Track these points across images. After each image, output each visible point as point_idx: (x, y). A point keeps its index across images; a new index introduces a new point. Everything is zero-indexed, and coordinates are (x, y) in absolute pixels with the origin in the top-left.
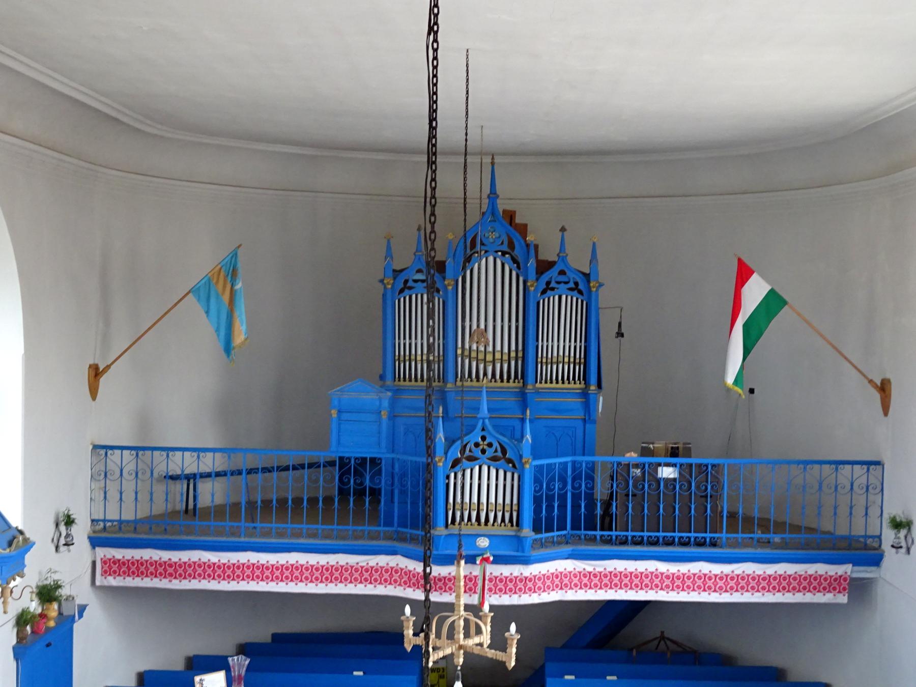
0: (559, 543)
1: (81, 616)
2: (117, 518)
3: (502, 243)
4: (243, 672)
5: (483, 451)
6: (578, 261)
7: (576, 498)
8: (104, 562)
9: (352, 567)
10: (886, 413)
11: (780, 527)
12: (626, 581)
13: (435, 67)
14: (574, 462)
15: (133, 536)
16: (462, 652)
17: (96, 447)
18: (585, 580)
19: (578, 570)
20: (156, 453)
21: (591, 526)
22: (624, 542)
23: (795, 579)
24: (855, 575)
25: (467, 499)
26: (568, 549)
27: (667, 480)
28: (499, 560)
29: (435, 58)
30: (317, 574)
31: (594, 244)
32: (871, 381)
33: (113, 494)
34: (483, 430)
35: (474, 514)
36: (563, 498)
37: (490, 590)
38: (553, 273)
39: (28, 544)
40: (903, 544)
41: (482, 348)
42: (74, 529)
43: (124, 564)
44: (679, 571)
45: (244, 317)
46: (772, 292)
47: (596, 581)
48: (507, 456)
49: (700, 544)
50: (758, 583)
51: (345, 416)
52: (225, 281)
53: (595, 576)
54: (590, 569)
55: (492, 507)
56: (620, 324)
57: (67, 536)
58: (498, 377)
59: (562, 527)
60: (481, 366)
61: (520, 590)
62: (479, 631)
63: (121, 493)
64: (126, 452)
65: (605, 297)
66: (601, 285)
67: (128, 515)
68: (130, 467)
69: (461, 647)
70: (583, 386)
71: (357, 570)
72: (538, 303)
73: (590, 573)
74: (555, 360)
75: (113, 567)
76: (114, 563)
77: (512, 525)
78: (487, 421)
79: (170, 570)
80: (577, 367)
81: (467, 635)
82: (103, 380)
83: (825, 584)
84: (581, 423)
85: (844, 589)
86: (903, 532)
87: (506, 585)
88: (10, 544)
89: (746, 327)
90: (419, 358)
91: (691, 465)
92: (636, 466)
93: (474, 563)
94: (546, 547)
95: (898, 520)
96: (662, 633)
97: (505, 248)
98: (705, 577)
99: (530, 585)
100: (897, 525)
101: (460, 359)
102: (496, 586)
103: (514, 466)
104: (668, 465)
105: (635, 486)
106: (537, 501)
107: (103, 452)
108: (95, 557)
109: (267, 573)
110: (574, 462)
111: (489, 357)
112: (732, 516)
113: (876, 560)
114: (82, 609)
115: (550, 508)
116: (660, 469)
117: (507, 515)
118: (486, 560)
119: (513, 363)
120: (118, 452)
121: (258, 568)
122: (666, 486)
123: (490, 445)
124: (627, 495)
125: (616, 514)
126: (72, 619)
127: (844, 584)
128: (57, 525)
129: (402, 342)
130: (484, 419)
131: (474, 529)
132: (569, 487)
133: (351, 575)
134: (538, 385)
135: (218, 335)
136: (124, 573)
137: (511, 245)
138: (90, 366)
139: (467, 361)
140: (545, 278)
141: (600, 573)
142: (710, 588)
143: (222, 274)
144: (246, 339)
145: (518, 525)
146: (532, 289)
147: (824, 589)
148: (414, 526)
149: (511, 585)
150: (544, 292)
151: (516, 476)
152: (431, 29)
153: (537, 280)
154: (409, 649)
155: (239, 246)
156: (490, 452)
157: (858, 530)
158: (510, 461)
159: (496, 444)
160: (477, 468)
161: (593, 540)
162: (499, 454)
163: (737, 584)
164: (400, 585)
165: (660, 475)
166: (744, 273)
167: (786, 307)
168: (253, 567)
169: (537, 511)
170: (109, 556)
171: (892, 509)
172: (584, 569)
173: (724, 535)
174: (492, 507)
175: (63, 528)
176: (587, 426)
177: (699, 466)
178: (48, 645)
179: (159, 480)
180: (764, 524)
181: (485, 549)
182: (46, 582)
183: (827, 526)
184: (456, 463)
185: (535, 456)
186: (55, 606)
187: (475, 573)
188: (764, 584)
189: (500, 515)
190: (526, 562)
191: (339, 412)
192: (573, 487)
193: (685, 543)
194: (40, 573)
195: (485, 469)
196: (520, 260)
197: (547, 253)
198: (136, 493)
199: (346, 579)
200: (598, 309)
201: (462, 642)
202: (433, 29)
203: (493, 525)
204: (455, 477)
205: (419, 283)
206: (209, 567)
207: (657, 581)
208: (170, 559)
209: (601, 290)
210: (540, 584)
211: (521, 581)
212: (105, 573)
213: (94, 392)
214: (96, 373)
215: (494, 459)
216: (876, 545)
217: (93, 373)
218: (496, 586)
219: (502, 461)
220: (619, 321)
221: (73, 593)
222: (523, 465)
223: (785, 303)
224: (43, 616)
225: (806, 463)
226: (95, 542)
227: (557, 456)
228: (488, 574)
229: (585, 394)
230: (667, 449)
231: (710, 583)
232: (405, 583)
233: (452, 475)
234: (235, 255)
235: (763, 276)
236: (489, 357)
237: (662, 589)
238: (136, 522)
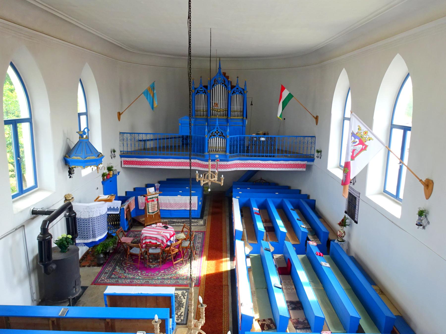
0: (236, 156)
1: (118, 174)
2: (127, 150)
3: (222, 81)
4: (159, 187)
5: (217, 134)
6: (241, 86)
7: (240, 145)
10: (317, 125)
11: (290, 152)
12: (252, 165)
13: (190, 28)
14: (240, 137)
15: (130, 155)
16: (210, 182)
17: (120, 133)
18: (242, 165)
20: (136, 134)
21: (244, 152)
22: (252, 156)
23: (293, 165)
24: (308, 164)
25: (213, 146)
26: (238, 158)
27: (263, 141)
28: (221, 160)
29: (190, 25)
31: (245, 81)
32: (313, 116)
33: (125, 145)
34: (217, 128)
35: (215, 149)
36: (237, 145)
37: (219, 168)
38: (235, 89)
39: (103, 156)
40: (319, 156)
41: (217, 108)
42: (116, 153)
43: (129, 162)
45: (156, 100)
46: (290, 93)
47: (245, 165)
48: (223, 135)
49: (270, 156)
50: (284, 166)
51: (182, 125)
52: (151, 91)
54: (243, 163)
56: (252, 102)
57: (114, 155)
58: (221, 115)
59: (237, 152)
60: (217, 113)
61: (226, 168)
62: (214, 177)
63: (127, 144)
64: (128, 134)
65: (248, 95)
66: (247, 92)
67: (129, 150)
68: (129, 138)
69: (210, 181)
70: (242, 118)
71: (186, 163)
72: (231, 96)
74: (235, 111)
75: (126, 163)
76: (126, 161)
78: (218, 126)
79: (140, 163)
81: (211, 178)
82: (122, 116)
83: (300, 166)
84: (241, 127)
85: (305, 167)
86: (319, 153)
87: (223, 167)
88: (98, 156)
89: (283, 102)
90: (201, 110)
91: (268, 137)
92: (255, 137)
93: (215, 161)
94: (233, 157)
95: (318, 150)
96: (261, 178)
97: (223, 82)
98: (271, 164)
99: (229, 166)
100: (318, 152)
101: (211, 111)
103: (225, 137)
104: (263, 137)
105: (255, 142)
106: (230, 146)
107: (122, 134)
109: (164, 164)
110: (240, 138)
111: (219, 110)
112: (278, 150)
113: (313, 160)
114: (119, 173)
115: (234, 148)
116: (261, 138)
117: (223, 150)
118: (218, 160)
119: (225, 112)
120: (126, 134)
121: (162, 163)
122: (262, 143)
123: (219, 132)
124: (253, 145)
126: (116, 175)
127: (305, 166)
128: (111, 152)
129: (197, 107)
130: (217, 126)
131: (215, 153)
132: (238, 143)
133: (185, 164)
134: (231, 117)
135: (150, 104)
136: (129, 164)
137: (224, 81)
138: (118, 112)
139: (213, 111)
140: (233, 90)
142: (272, 167)
143: (150, 89)
144: (157, 105)
145: (226, 152)
146: (230, 93)
147: (300, 167)
148: (200, 152)
150: (233, 94)
151: (225, 140)
152: (189, 17)
153: (231, 90)
154: (197, 181)
155: (155, 82)
156: (219, 134)
157: (309, 153)
158: (224, 136)
159: (220, 132)
160: (216, 138)
161: (244, 156)
162: (221, 134)
163: (279, 166)
165: (261, 140)
166: (283, 89)
167: (293, 98)
168: (161, 162)
169: (230, 148)
171: (317, 148)
173: (276, 154)
175: (113, 153)
176: (244, 128)
177: (270, 137)
178: (111, 181)
179: (137, 141)
180: (286, 152)
181: (217, 158)
182: (109, 166)
183: (301, 152)
184: (211, 136)
185: (230, 135)
186: (112, 172)
188: (285, 166)
189: (221, 149)
190: (228, 161)
191: (181, 124)
192: (239, 143)
193: (267, 156)
194: (108, 164)
195: (218, 138)
196: (227, 85)
197: (234, 84)
198: (131, 144)
200: (246, 98)
201: (210, 179)
202: (189, 17)
205: (201, 91)
206: (150, 162)
207: (260, 165)
209: (247, 93)
210: (231, 166)
211: (226, 165)
212: (124, 164)
213: (119, 119)
214: (119, 114)
215: (220, 136)
216: (313, 157)
217: (119, 114)
219: (222, 136)
221: (116, 169)
222: (227, 137)
223: (293, 96)
224: (109, 174)
225: (297, 137)
226: (121, 156)
227: (236, 135)
228: (218, 164)
229: (243, 120)
230: (263, 134)
231: (272, 166)
232: (198, 166)
233: (209, 140)
234: (154, 84)
235: (288, 90)
236: (219, 110)
238: (131, 152)
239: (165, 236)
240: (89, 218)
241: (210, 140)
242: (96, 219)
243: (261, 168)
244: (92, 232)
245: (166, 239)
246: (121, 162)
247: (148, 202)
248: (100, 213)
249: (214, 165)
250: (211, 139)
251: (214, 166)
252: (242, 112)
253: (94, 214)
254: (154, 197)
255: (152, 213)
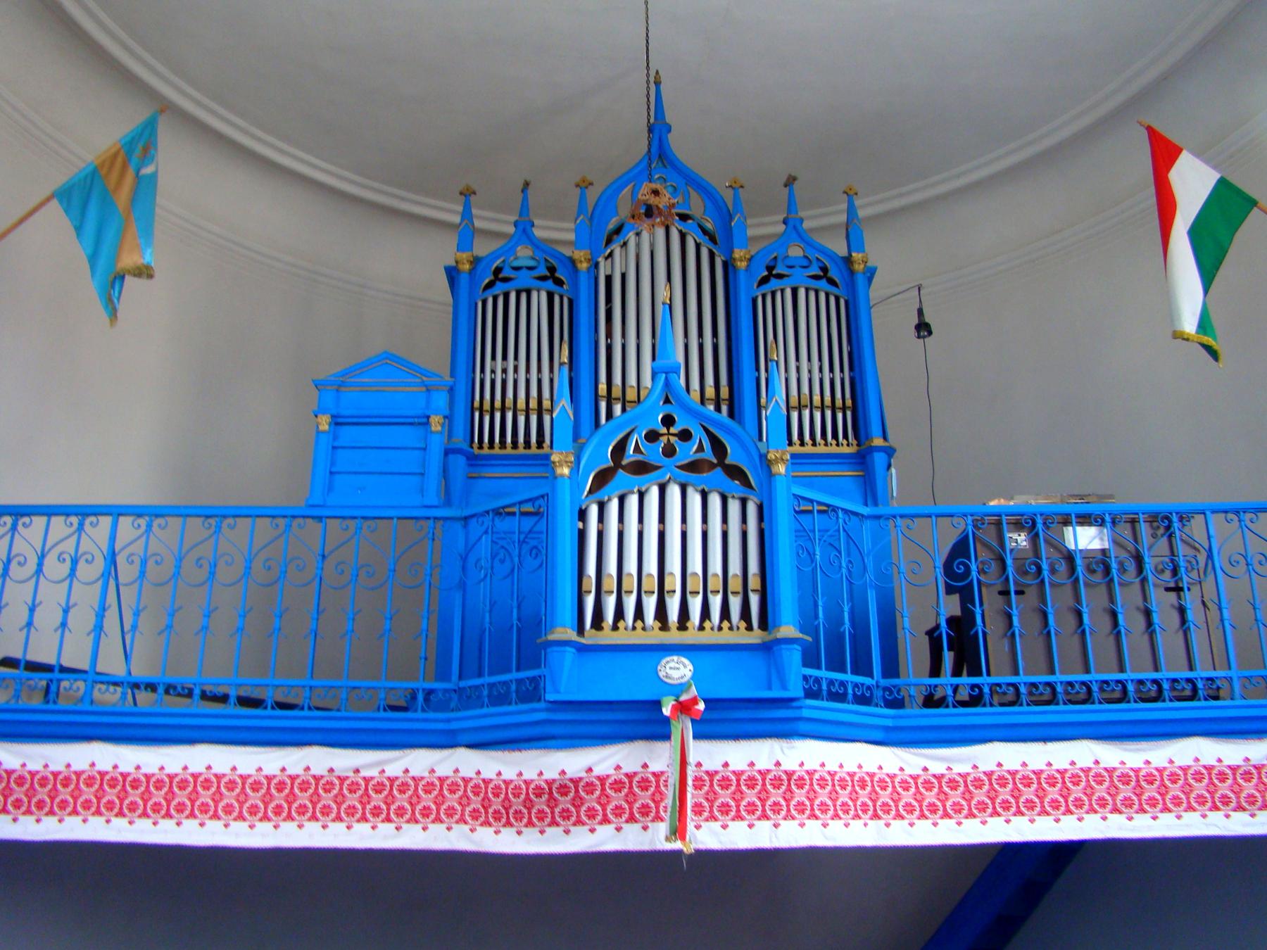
9: (342, 780)
18: (930, 797)
19: (909, 771)
25: (631, 566)
27: (1087, 553)
30: (255, 798)
34: (667, 401)
35: (650, 604)
37: (698, 809)
44: (1148, 762)
46: (1222, 183)
47: (956, 796)
48: (728, 461)
51: (349, 435)
53: (953, 784)
54: (937, 768)
55: (695, 584)
61: (776, 808)
72: (754, 301)
73: (939, 778)
77: (749, 628)
80: (840, 416)
87: (738, 795)
89: (1195, 233)
98: (1212, 774)
99: (800, 795)
102: (711, 797)
103: (746, 483)
116: (1068, 531)
117: (735, 604)
123: (685, 435)
125: (984, 634)
141: (964, 776)
142: (1225, 801)
149: (751, 796)
156: (687, 452)
158: (736, 473)
159: (698, 434)
160: (655, 491)
162: (708, 454)
164: (462, 820)
172: (925, 769)
174: (695, 584)
181: (684, 687)
184: (603, 478)
187: (655, 767)
189: (716, 602)
191: (337, 422)
195: (674, 492)
199: (326, 811)
203: (701, 628)
204: (601, 518)
210: (823, 796)
211: (777, 782)
215: (693, 467)
218: (711, 797)
219: (719, 470)
220: (917, 306)
223: (1254, 203)
228: (692, 758)
229: (862, 459)
232: (475, 815)
233: (594, 511)
237: (1116, 810)
241: (601, 518)
243: (1115, 818)
249: (644, 784)
250: (614, 506)
251: (644, 798)
252: (844, 409)
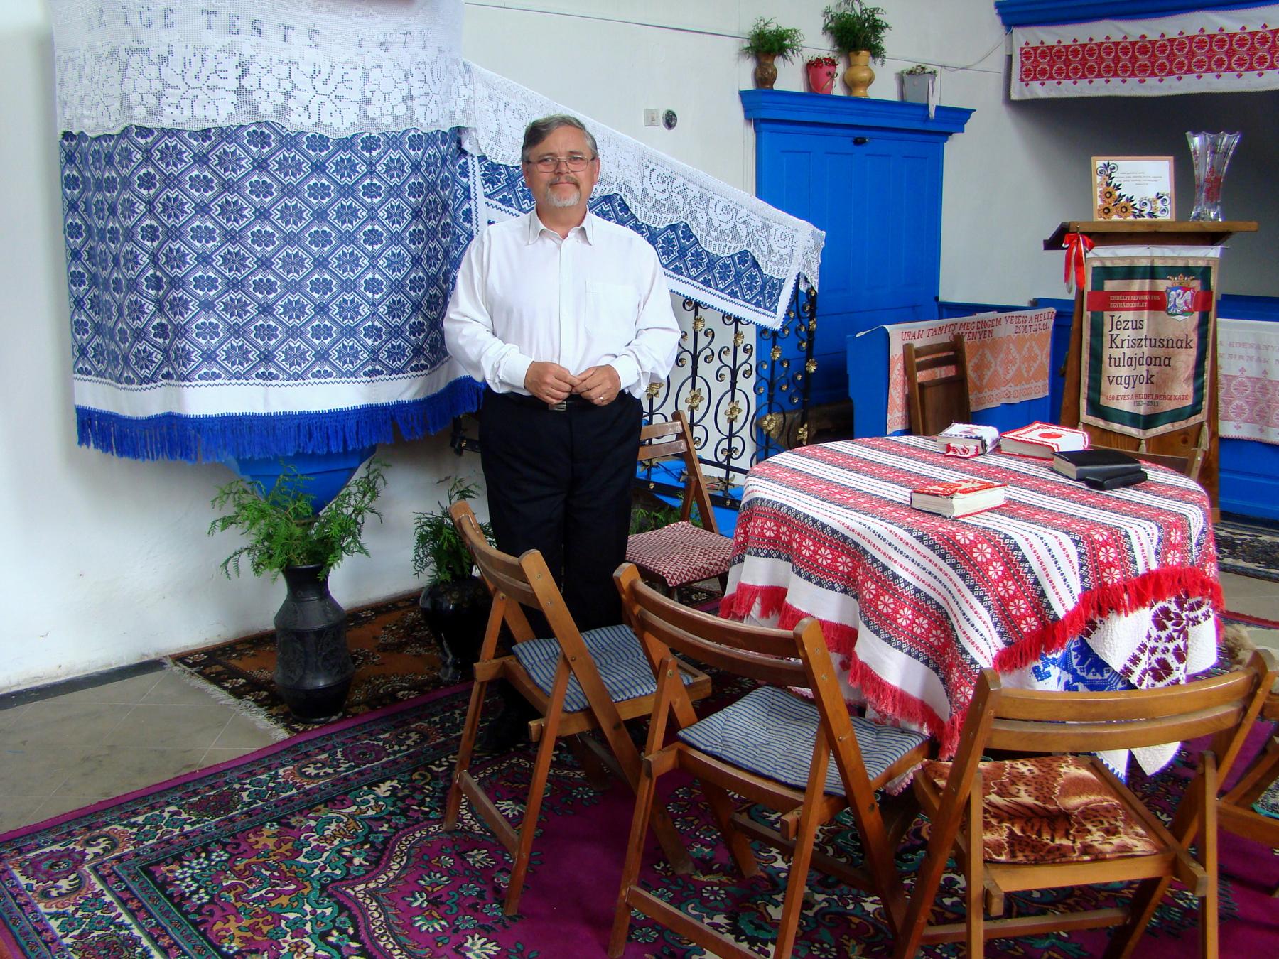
8: (1026, 55)
108: (1011, 48)
170: (1035, 43)
208: (1143, 37)
212: (1027, 75)
239: (983, 553)
240: (125, 133)
242: (201, 159)
244: (160, 309)
245: (1006, 620)
246: (1010, 57)
247: (1104, 302)
248: (243, 94)
253: (172, 95)
254: (1171, 271)
255: (1134, 420)
